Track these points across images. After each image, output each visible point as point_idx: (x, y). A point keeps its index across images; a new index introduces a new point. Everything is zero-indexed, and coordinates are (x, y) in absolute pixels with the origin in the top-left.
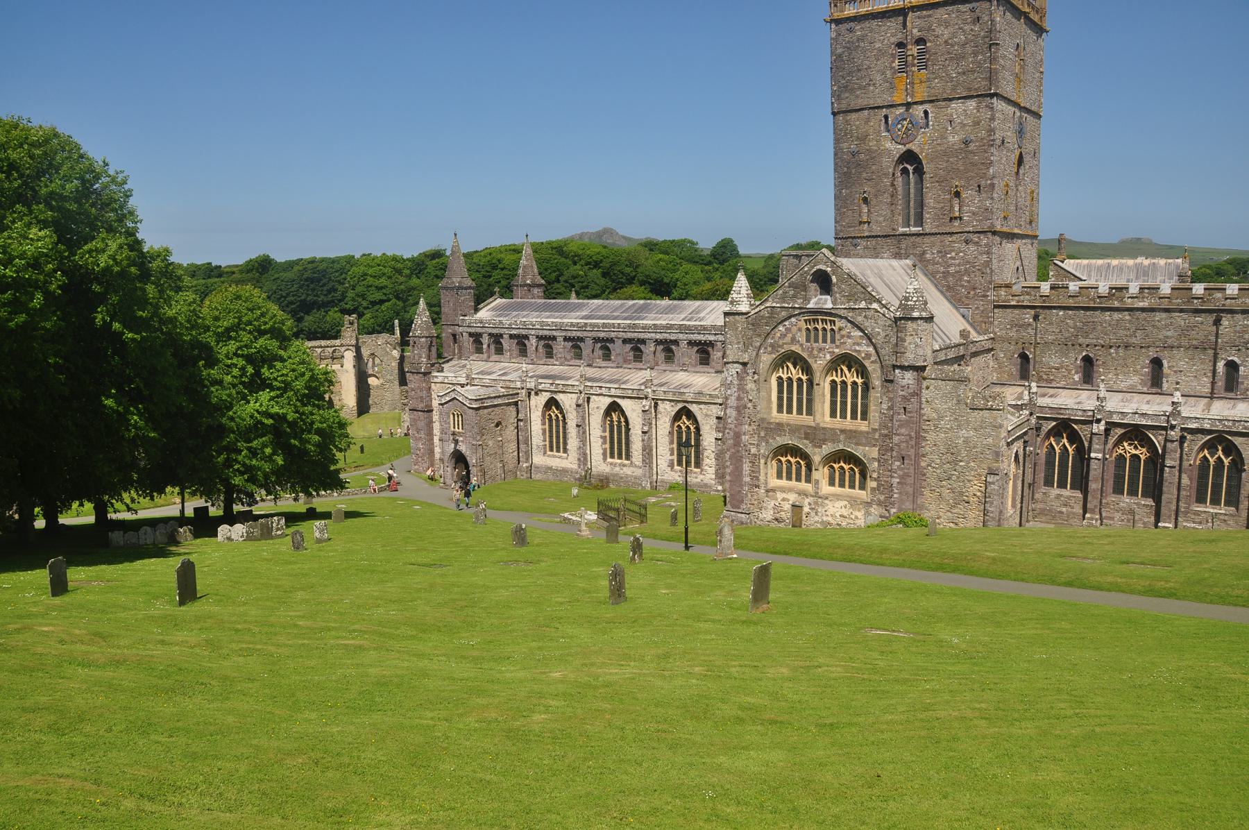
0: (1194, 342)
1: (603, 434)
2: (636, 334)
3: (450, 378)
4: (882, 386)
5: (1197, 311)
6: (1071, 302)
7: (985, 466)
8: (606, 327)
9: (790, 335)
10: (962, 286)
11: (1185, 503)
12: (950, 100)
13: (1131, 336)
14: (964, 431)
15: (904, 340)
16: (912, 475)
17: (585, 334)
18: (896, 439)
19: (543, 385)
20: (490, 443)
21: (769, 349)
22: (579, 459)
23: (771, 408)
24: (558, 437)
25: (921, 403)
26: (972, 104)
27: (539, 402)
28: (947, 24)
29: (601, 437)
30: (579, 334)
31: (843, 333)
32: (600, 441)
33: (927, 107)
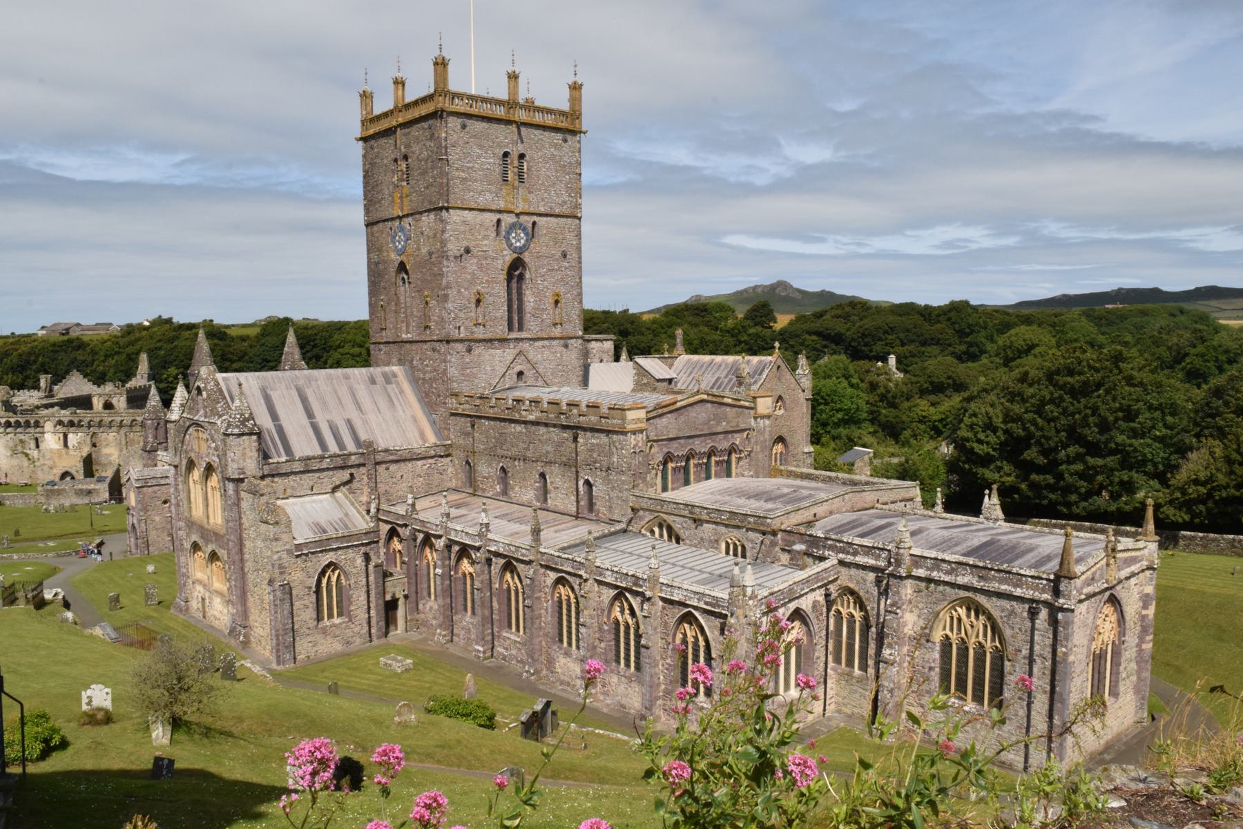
0: (564, 459)
5: (565, 427)
6: (491, 412)
12: (421, 213)
15: (226, 454)
18: (230, 543)
20: (157, 519)
23: (190, 508)
25: (240, 513)
26: (432, 216)
28: (417, 140)
33: (410, 219)
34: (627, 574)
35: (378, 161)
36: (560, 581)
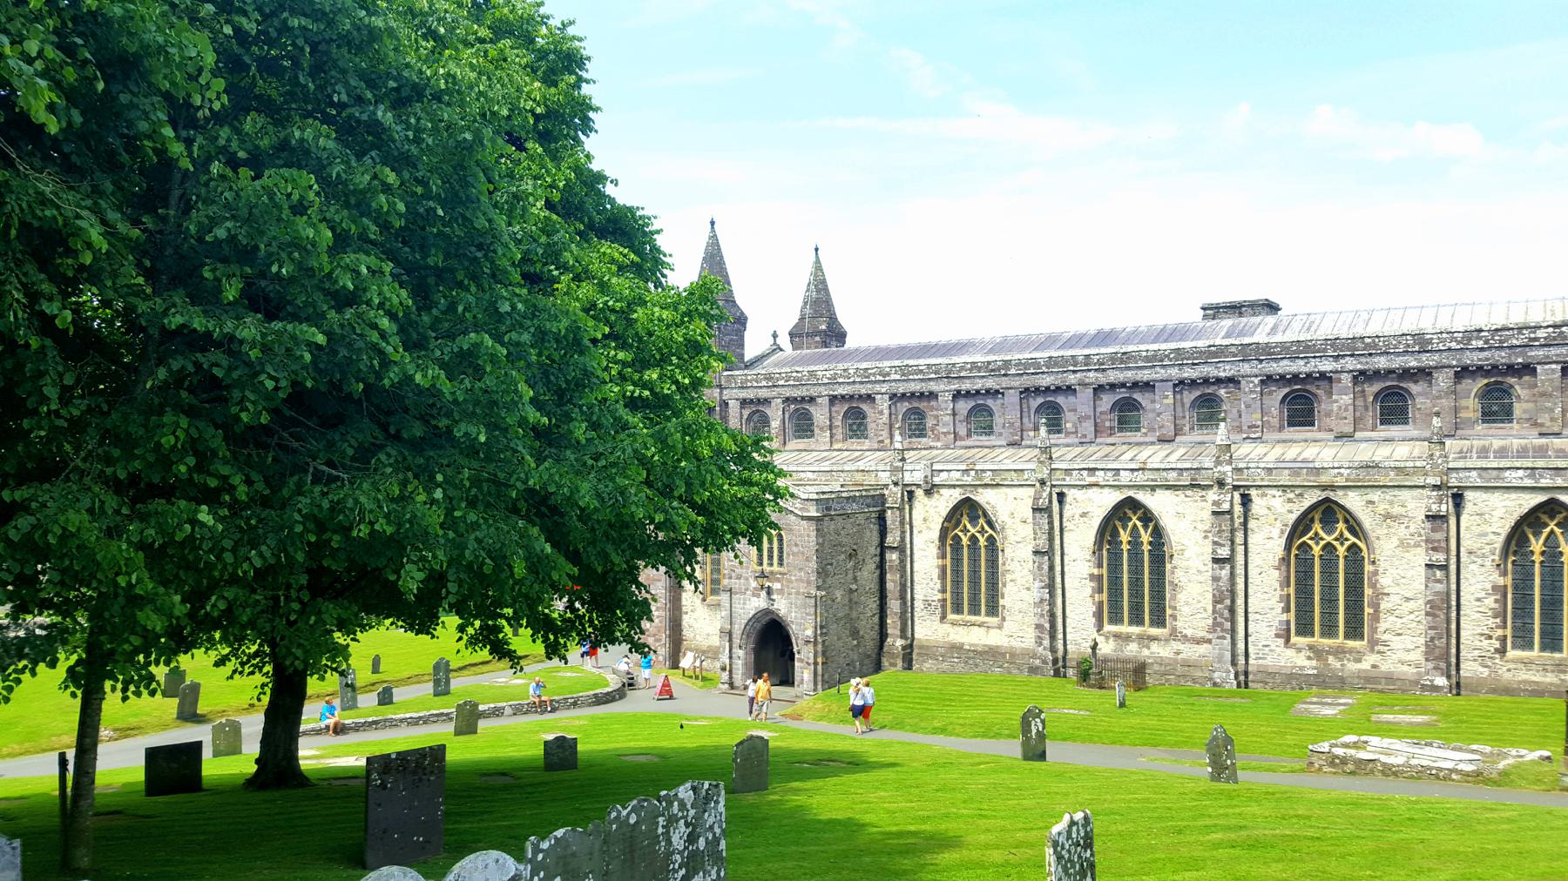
1: (1096, 571)
2: (1129, 374)
8: (1056, 364)
17: (1005, 382)
19: (944, 475)
22: (1038, 627)
24: (975, 583)
29: (1092, 577)
30: (991, 383)
32: (1089, 586)
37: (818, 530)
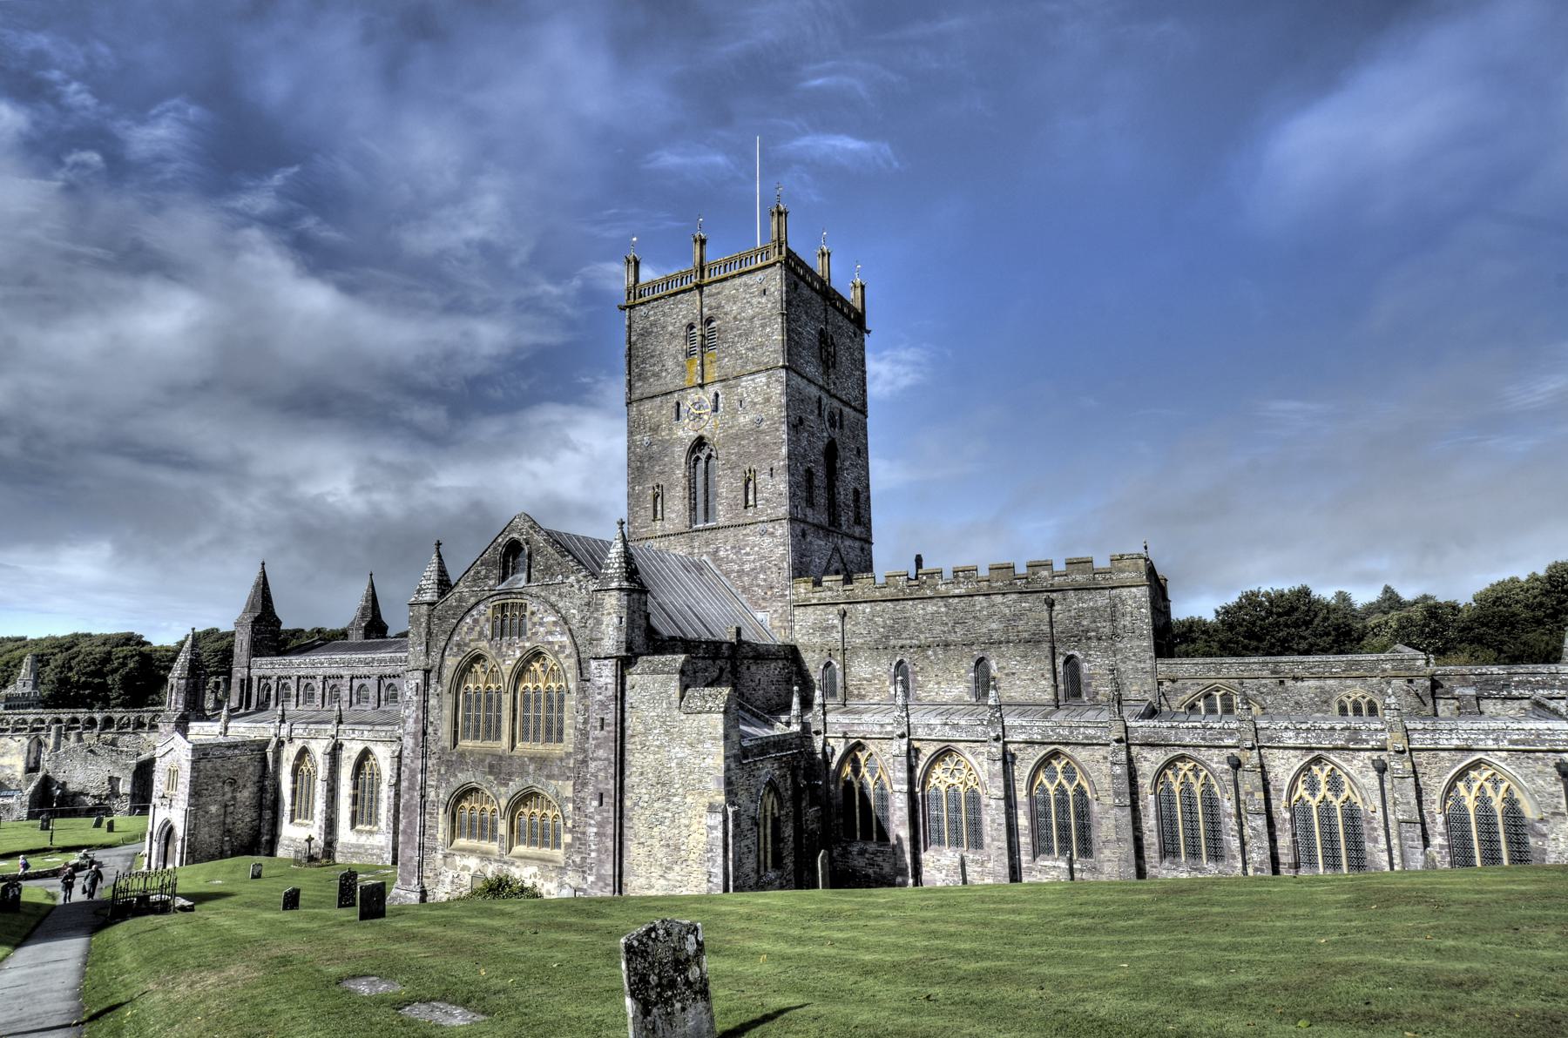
0: (1026, 635)
3: (206, 729)
4: (578, 689)
7: (705, 800)
9: (478, 629)
10: (758, 586)
11: (1027, 854)
13: (950, 632)
14: (677, 749)
15: (599, 622)
16: (612, 820)
18: (593, 765)
21: (455, 649)
22: (320, 827)
26: (761, 379)
27: (290, 753)
28: (734, 299)
31: (535, 619)
33: (717, 387)
34: (1332, 729)
35: (655, 330)
36: (1170, 764)
37: (193, 768)
